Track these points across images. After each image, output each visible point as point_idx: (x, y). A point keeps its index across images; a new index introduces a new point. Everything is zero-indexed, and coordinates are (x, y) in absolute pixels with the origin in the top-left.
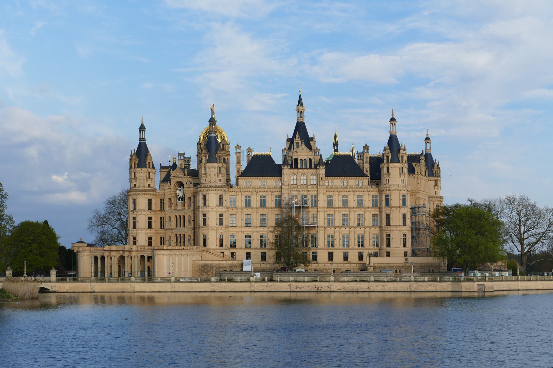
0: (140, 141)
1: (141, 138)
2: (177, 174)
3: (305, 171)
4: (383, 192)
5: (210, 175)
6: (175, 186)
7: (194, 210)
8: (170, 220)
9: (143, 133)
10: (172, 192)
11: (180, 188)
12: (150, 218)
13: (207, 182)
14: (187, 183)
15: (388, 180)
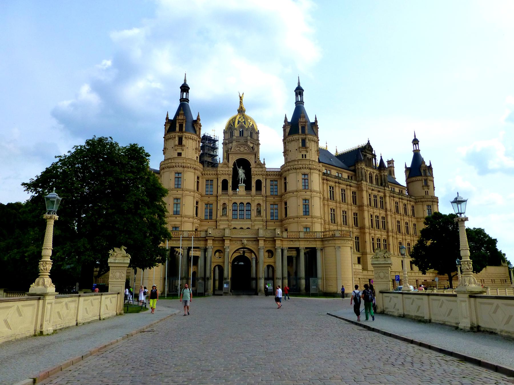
0: (180, 102)
1: (184, 97)
2: (239, 149)
3: (372, 170)
4: (424, 203)
5: (311, 150)
6: (234, 165)
7: (266, 197)
8: (224, 208)
9: (183, 94)
10: (231, 171)
11: (239, 168)
12: (197, 203)
13: (308, 158)
14: (255, 162)
15: (427, 192)
